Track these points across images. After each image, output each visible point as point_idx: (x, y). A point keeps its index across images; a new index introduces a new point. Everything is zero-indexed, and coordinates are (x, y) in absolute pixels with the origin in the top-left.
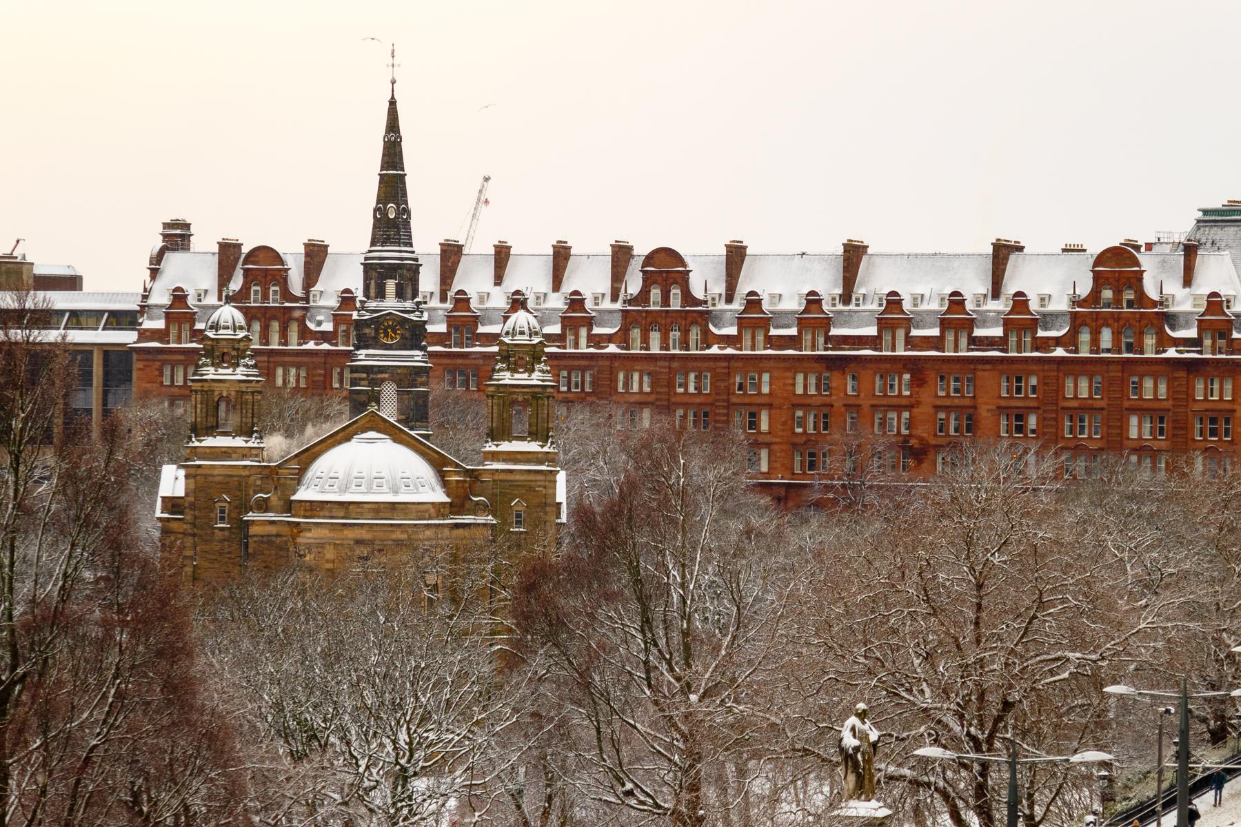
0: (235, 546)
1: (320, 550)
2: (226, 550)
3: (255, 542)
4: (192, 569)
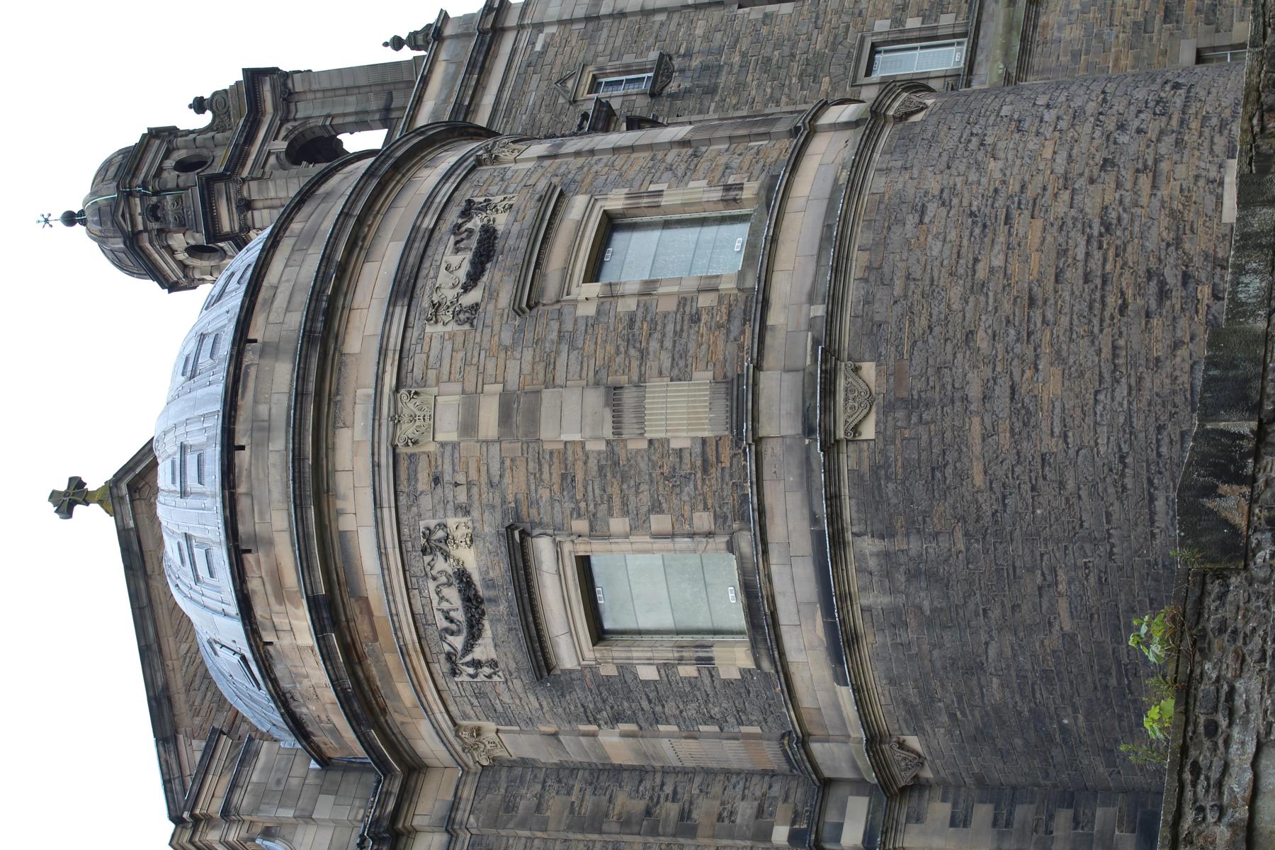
1: (423, 482)
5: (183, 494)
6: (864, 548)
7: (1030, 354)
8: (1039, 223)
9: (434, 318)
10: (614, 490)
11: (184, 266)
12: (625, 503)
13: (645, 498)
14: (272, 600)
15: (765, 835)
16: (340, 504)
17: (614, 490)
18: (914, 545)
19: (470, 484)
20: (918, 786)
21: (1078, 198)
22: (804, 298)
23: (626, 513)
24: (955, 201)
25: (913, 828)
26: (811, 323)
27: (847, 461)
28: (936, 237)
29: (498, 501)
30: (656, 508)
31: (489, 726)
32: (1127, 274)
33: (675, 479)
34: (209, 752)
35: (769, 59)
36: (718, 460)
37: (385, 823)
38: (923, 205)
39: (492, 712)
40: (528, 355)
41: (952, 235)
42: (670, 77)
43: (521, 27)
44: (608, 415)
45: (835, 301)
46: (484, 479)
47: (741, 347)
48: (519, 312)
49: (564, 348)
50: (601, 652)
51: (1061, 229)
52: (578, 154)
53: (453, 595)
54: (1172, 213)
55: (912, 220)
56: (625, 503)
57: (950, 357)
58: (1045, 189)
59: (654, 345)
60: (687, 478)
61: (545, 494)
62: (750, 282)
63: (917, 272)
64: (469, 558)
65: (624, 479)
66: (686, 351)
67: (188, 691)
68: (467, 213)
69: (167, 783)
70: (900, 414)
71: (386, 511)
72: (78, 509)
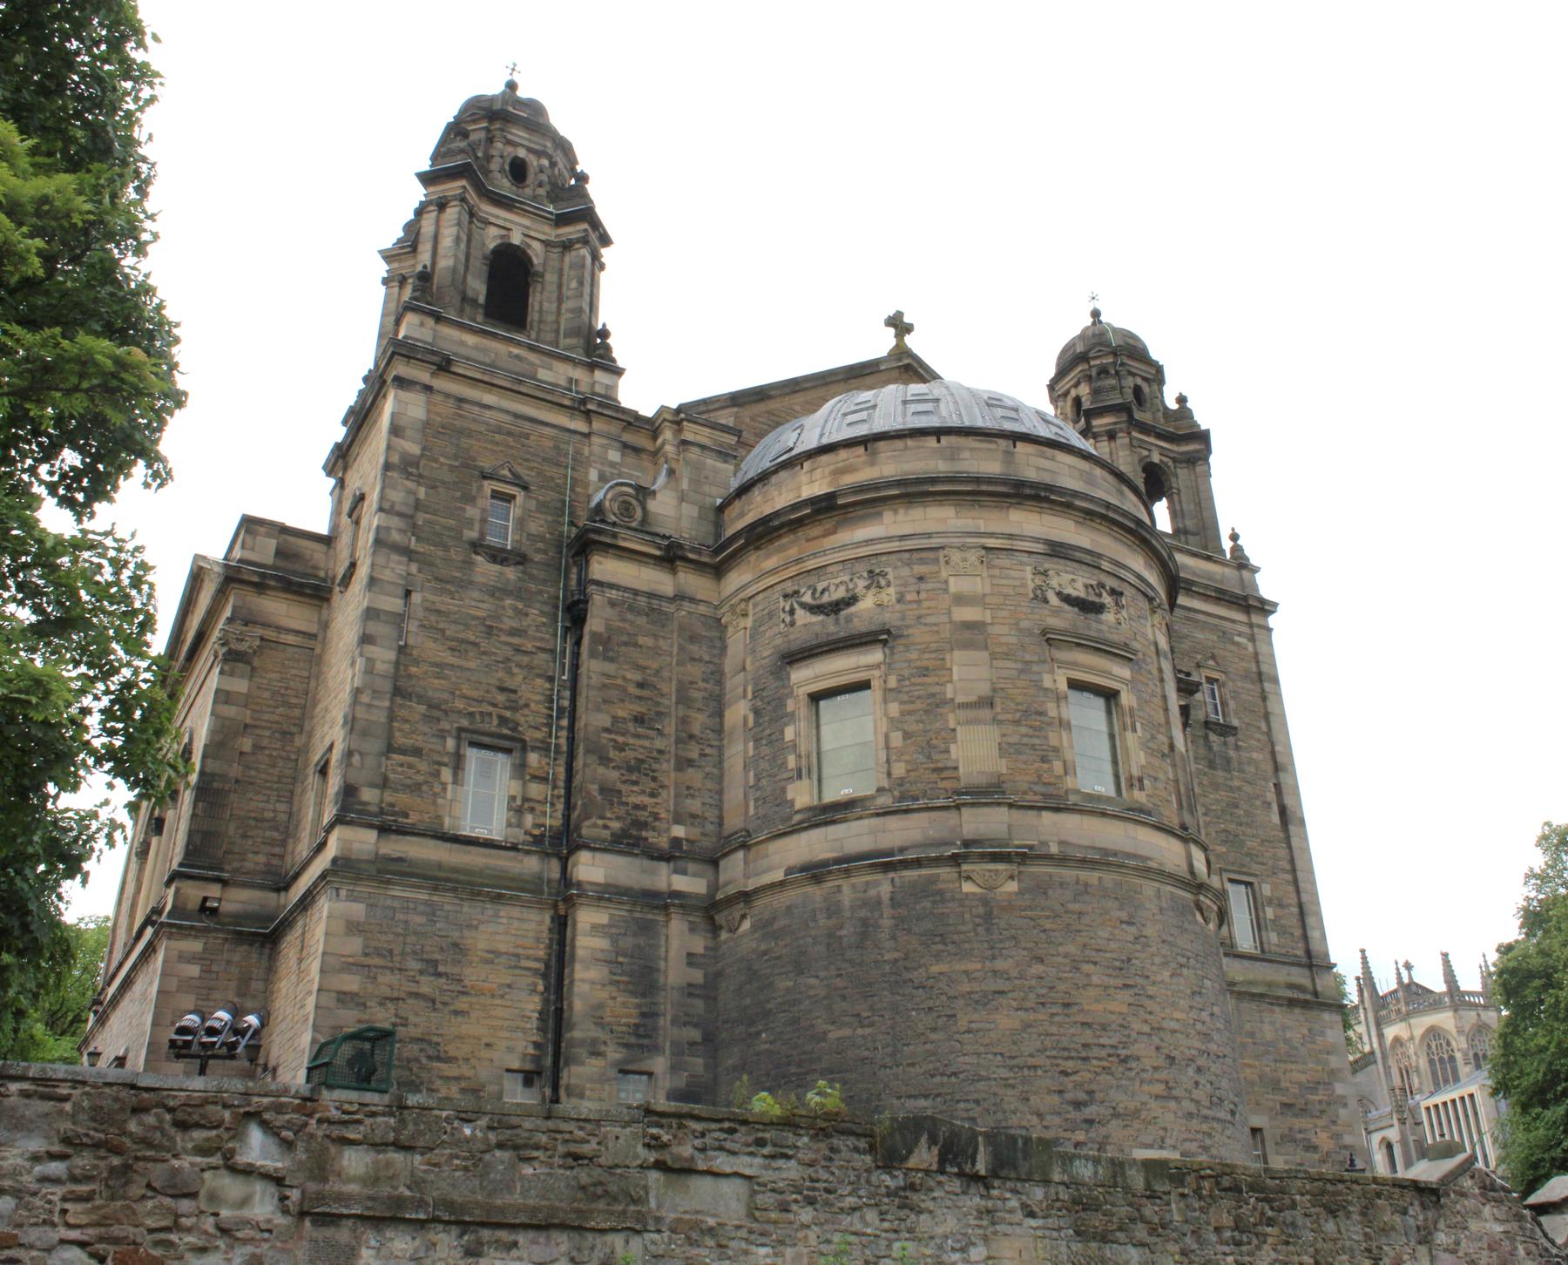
0: (535, 616)
2: (509, 623)
3: (612, 604)
4: (391, 655)
5: (905, 402)
6: (884, 886)
7: (1028, 1004)
8: (1125, 1009)
9: (1037, 572)
10: (919, 705)
11: (1066, 394)
12: (910, 713)
13: (913, 728)
14: (832, 467)
15: (678, 820)
16: (901, 511)
17: (919, 705)
18: (886, 922)
19: (919, 602)
20: (715, 929)
21: (1145, 1038)
22: (1062, 838)
23: (902, 714)
24: (1138, 947)
25: (685, 926)
26: (1045, 844)
27: (945, 872)
28: (1112, 934)
29: (908, 622)
30: (907, 735)
31: (749, 622)
32: (1090, 1076)
33: (928, 749)
34: (725, 429)
35: (1237, 807)
36: (943, 779)
37: (680, 553)
38: (1133, 924)
39: (759, 623)
40: (1013, 640)
41: (1113, 945)
42: (1221, 735)
43: (1251, 626)
44: (973, 698)
45: (1062, 860)
46: (923, 612)
47: (1025, 793)
48: (1044, 632)
49: (1019, 666)
50: (804, 699)
51: (1122, 1026)
52: (1160, 670)
53: (840, 593)
54: (1137, 1112)
55: (1124, 915)
56: (910, 713)
57: (1023, 945)
58: (1150, 1013)
59: (1023, 730)
60: (929, 757)
61: (914, 656)
62: (1073, 799)
63: (1086, 920)
64: (866, 604)
65: (927, 712)
66: (1020, 753)
67: (768, 412)
68: (1113, 592)
69: (705, 402)
70: (981, 910)
71: (897, 544)
72: (892, 331)
